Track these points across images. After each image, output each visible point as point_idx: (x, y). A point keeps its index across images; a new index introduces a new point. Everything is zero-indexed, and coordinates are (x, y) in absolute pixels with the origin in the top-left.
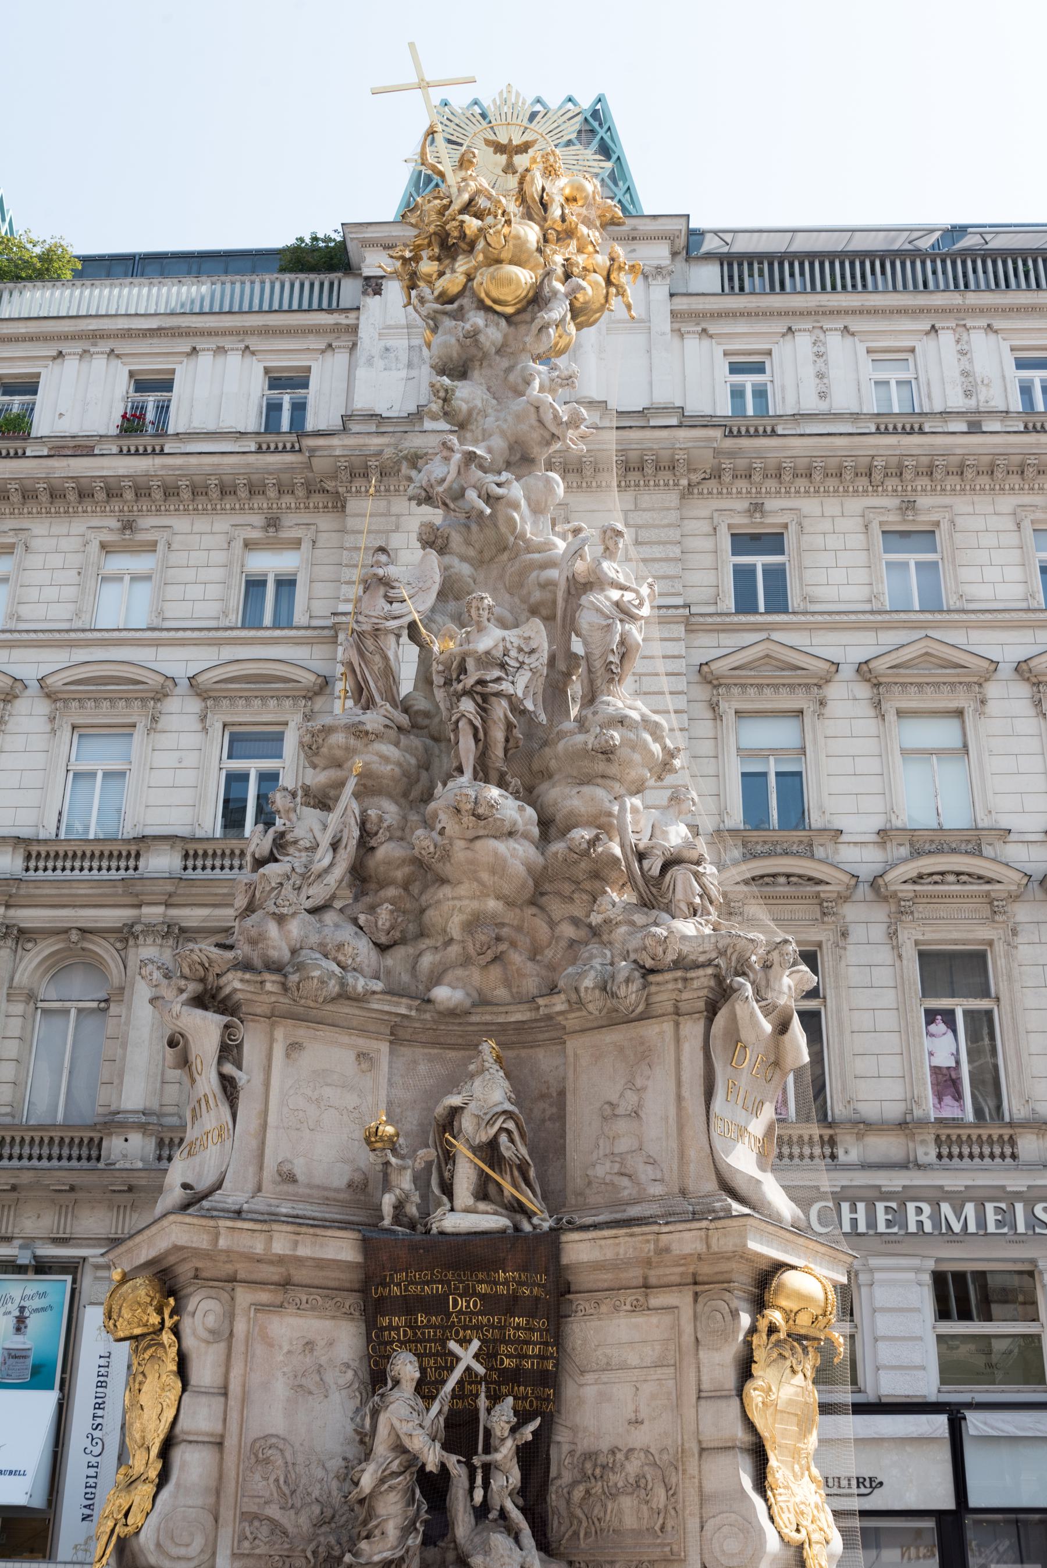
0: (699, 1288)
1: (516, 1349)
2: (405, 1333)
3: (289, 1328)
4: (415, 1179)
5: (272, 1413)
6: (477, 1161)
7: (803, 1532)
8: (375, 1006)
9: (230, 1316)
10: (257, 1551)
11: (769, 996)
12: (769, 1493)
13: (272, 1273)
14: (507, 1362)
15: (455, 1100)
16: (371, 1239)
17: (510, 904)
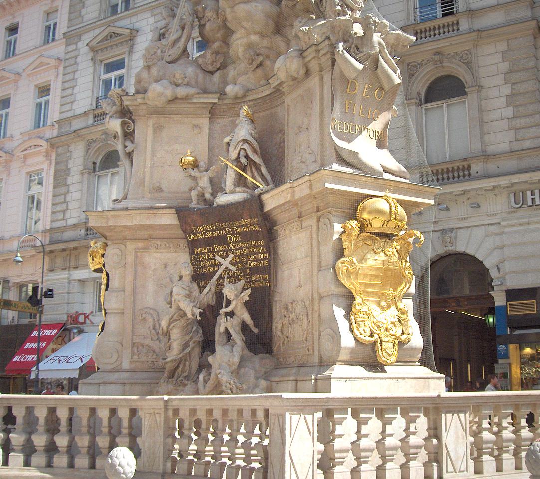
0: (319, 214)
1: (255, 258)
2: (208, 255)
3: (155, 259)
4: (211, 180)
5: (151, 297)
6: (234, 167)
7: (376, 337)
8: (195, 101)
9: (124, 255)
10: (141, 360)
11: (365, 50)
12: (352, 317)
13: (144, 233)
14: (252, 264)
15: (227, 140)
16: (182, 212)
17: (262, 35)
